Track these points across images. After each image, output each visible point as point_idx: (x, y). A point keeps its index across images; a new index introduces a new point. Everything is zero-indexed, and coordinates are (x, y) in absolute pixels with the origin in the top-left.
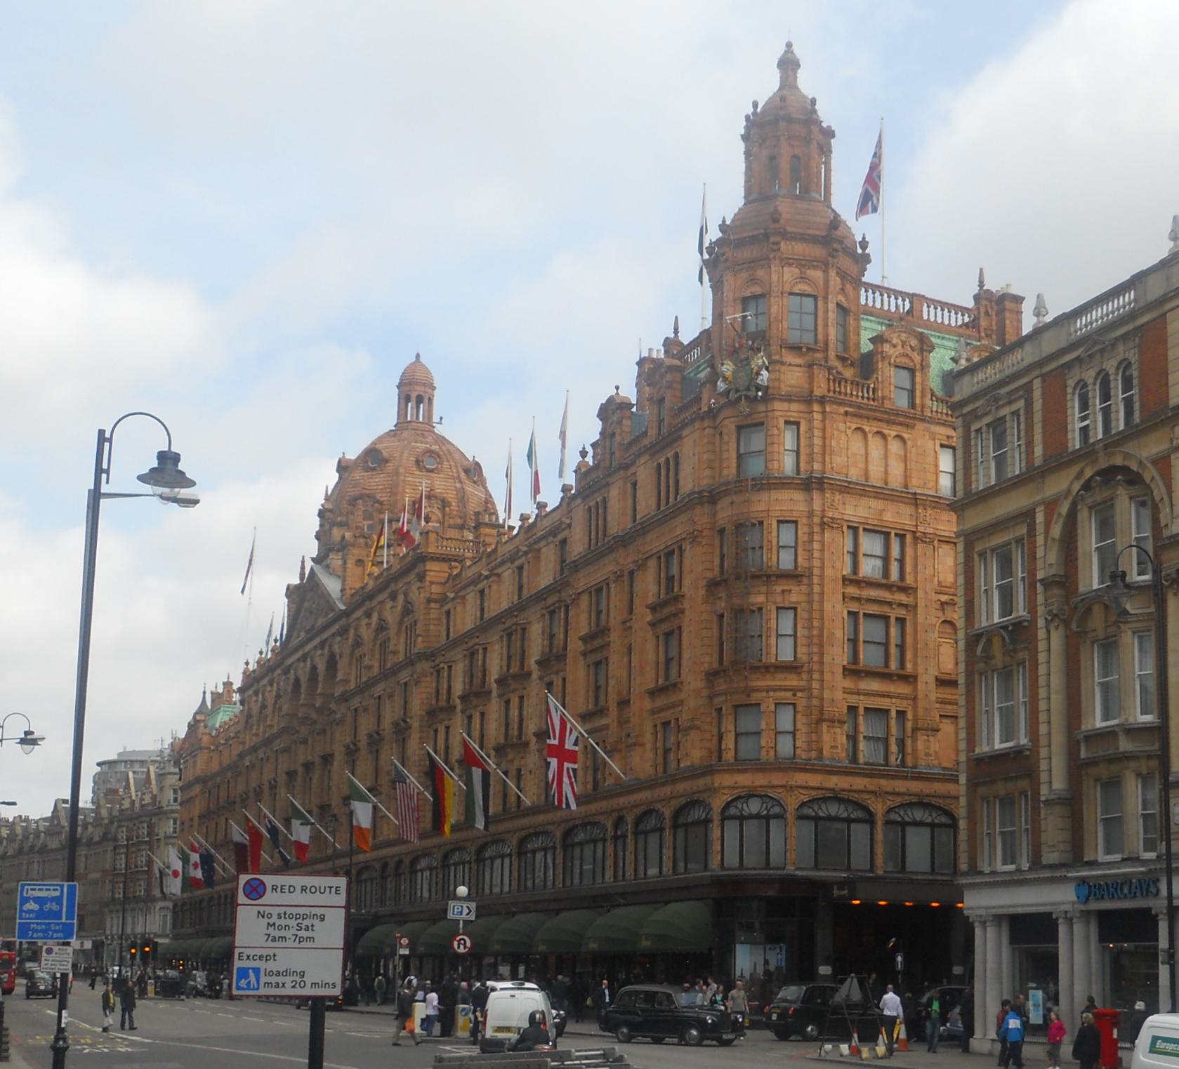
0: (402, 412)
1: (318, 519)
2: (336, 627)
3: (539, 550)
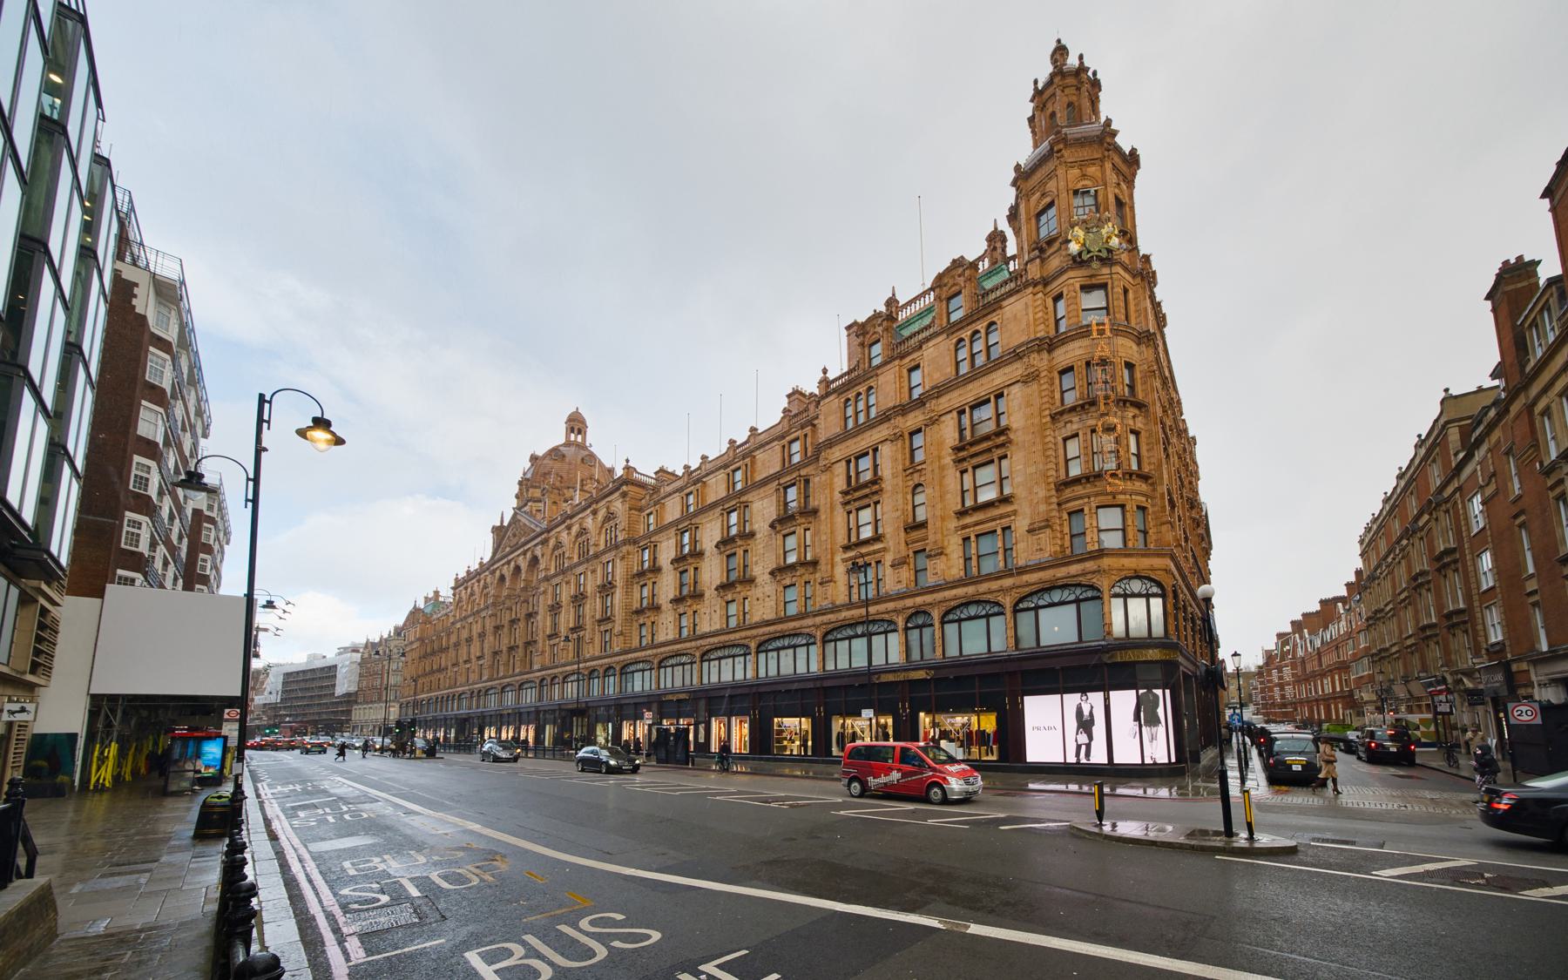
0: (568, 436)
1: (518, 486)
2: (539, 539)
3: (754, 457)
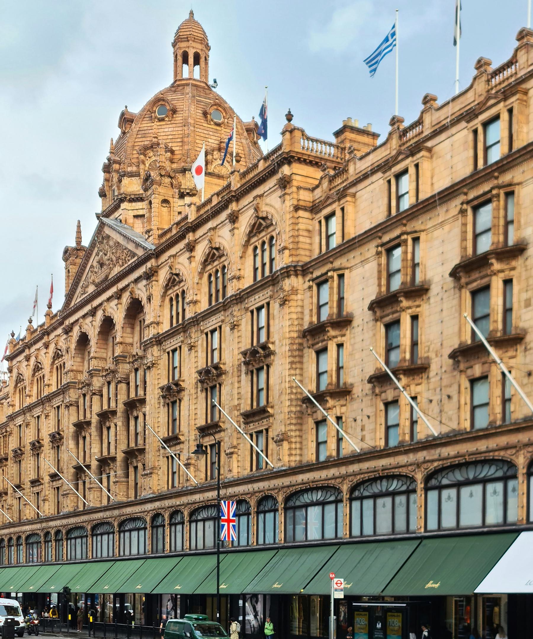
2: (142, 270)
